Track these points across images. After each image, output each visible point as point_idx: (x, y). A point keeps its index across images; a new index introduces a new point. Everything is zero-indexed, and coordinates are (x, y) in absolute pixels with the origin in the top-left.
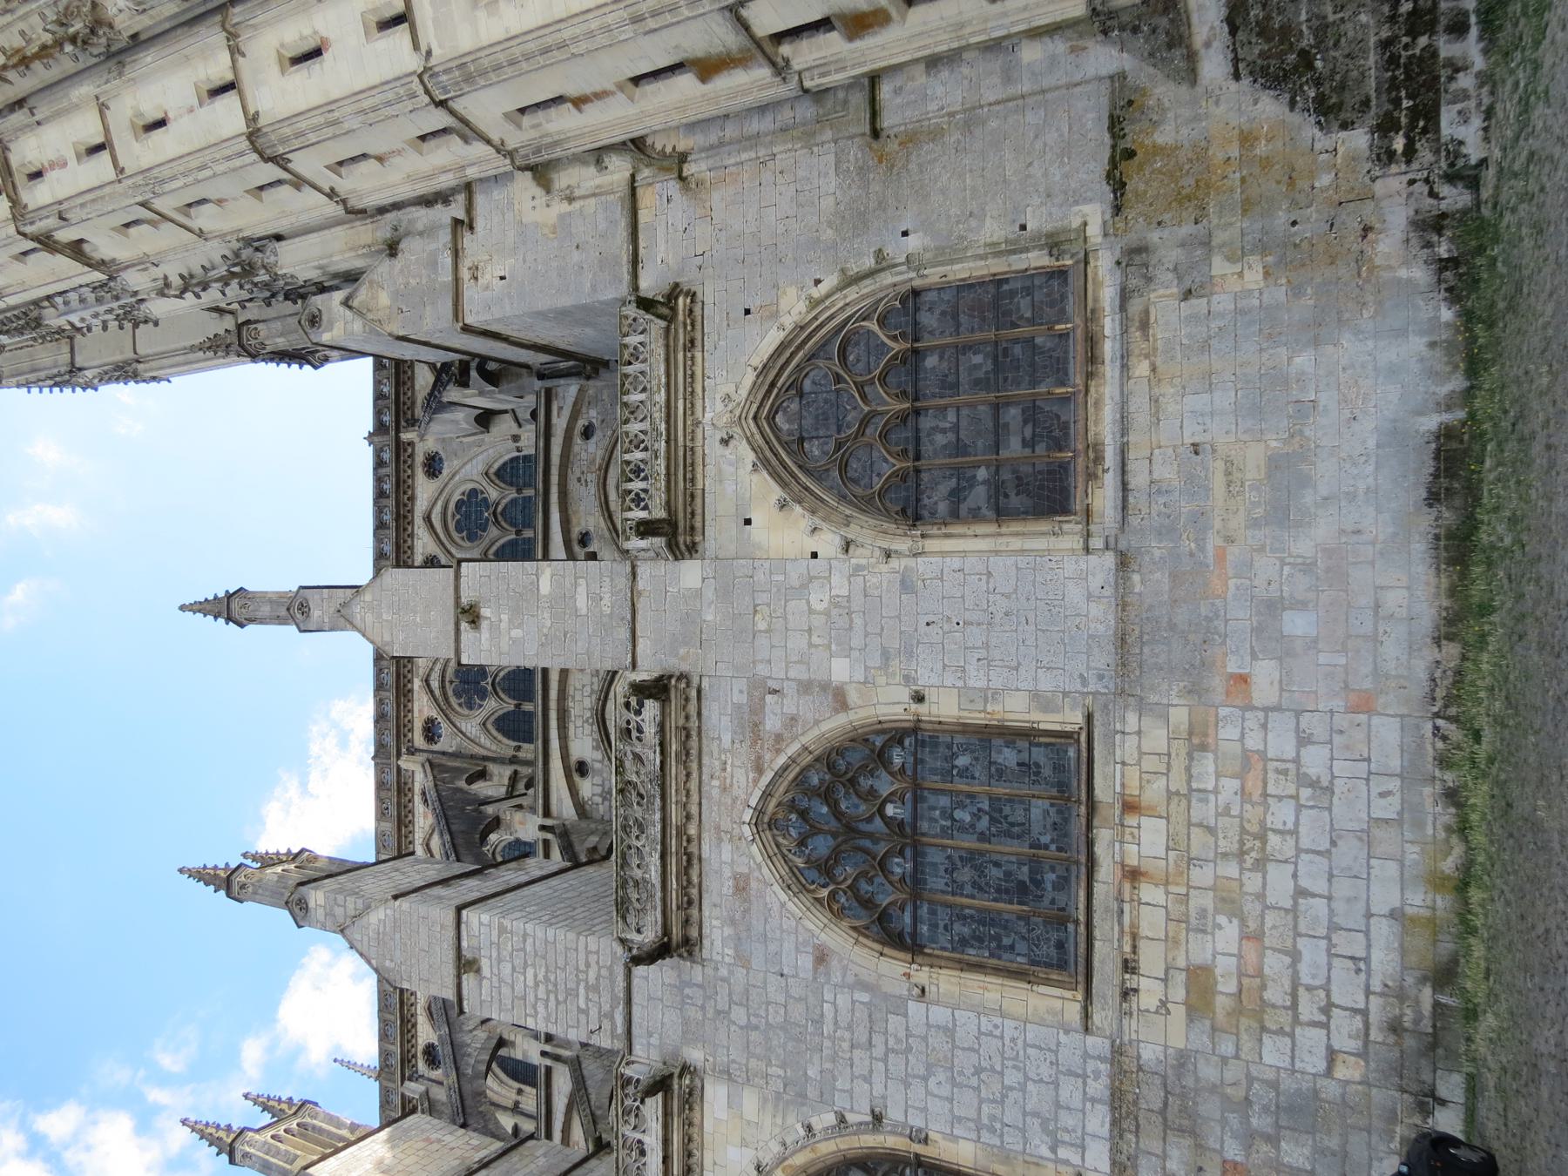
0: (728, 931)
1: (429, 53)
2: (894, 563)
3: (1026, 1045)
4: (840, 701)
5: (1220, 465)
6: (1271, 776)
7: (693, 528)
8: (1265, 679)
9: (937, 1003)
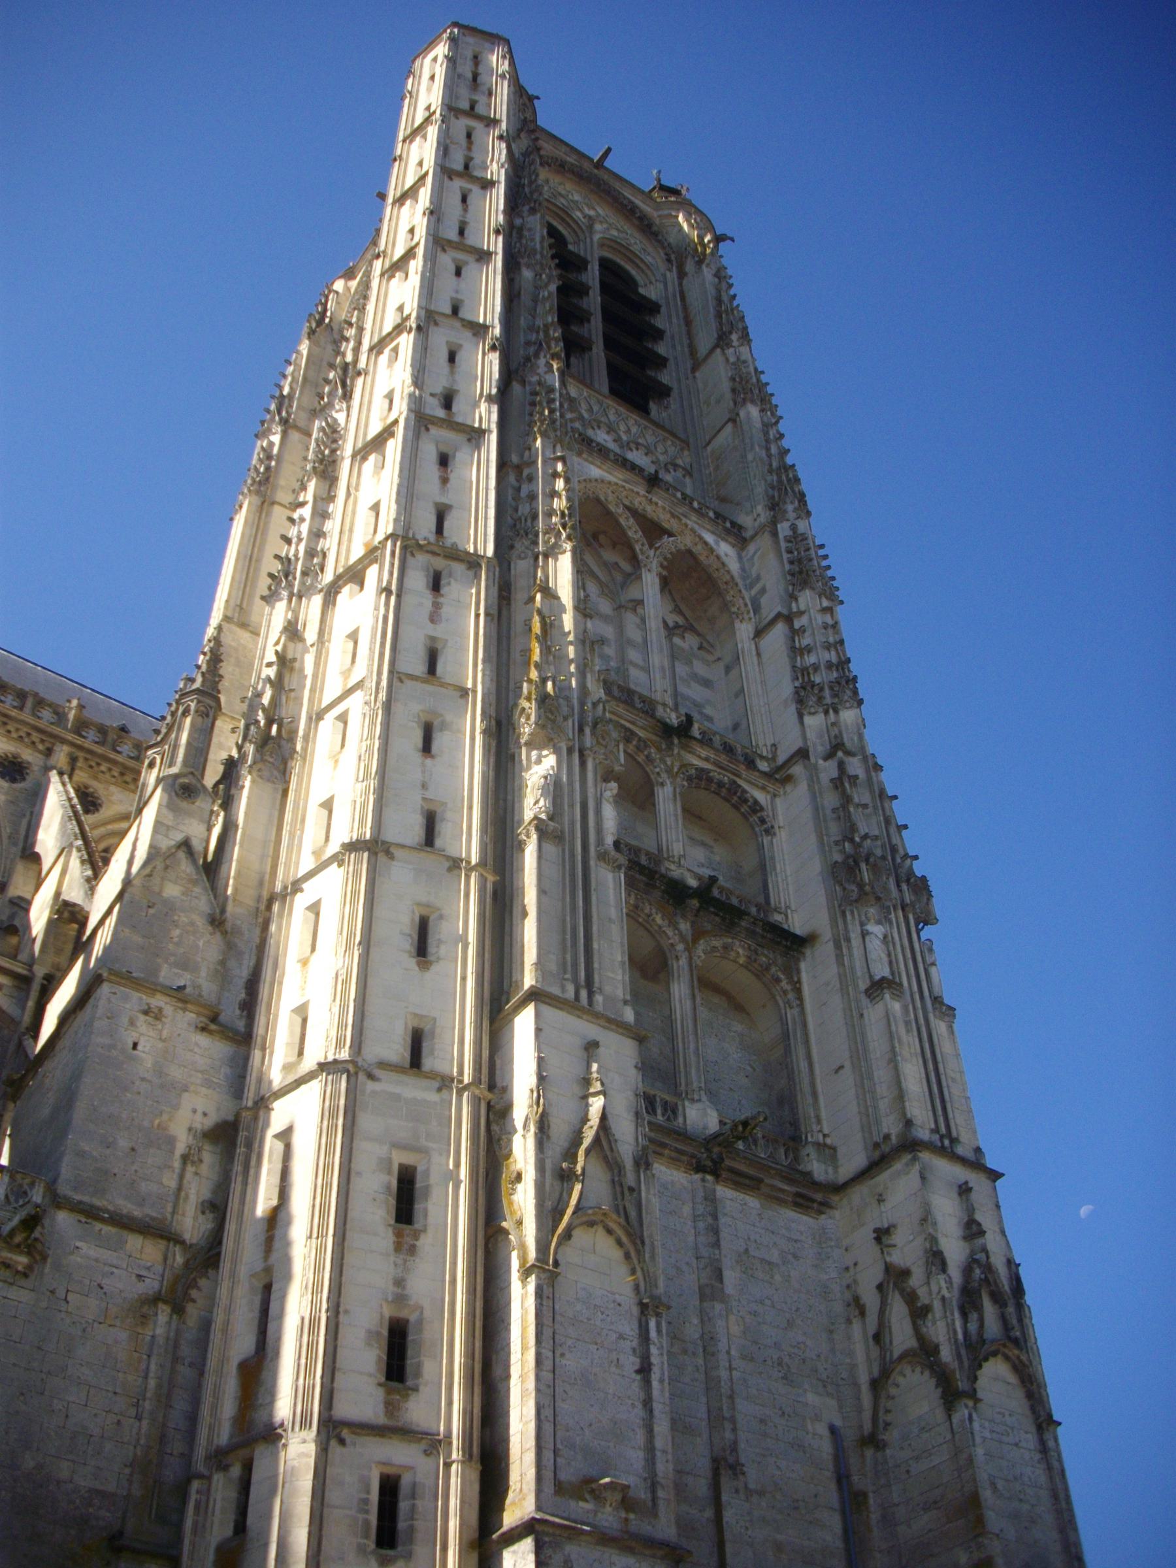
1: (371, 1076)
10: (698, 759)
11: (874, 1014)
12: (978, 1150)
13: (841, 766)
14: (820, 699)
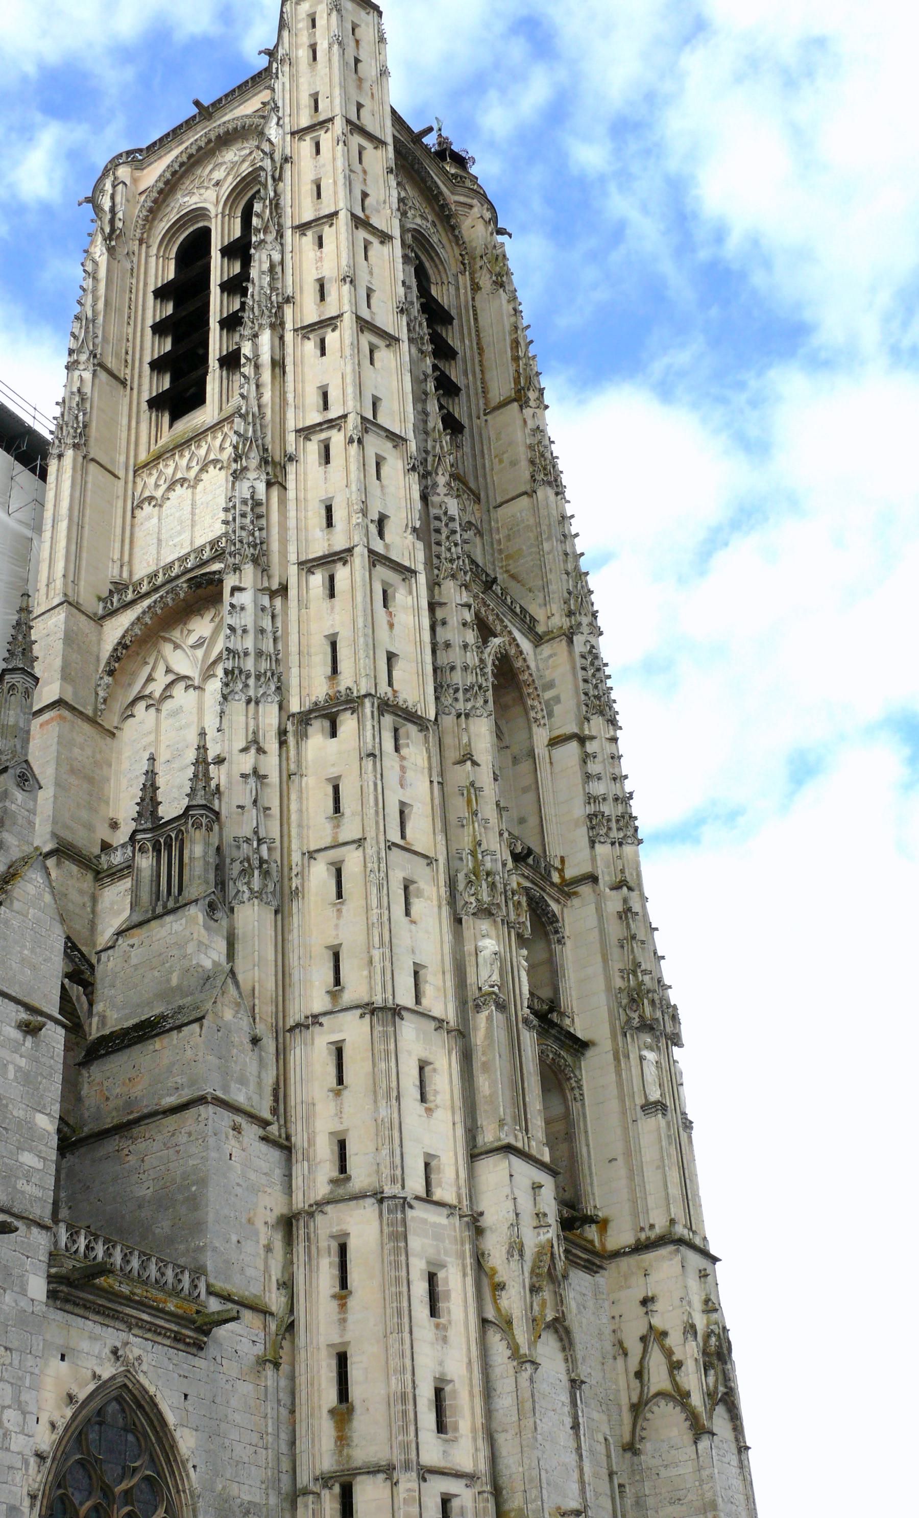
1: (411, 1207)
2: (27, 1502)
7: (67, 1301)
12: (705, 1239)
13: (625, 901)
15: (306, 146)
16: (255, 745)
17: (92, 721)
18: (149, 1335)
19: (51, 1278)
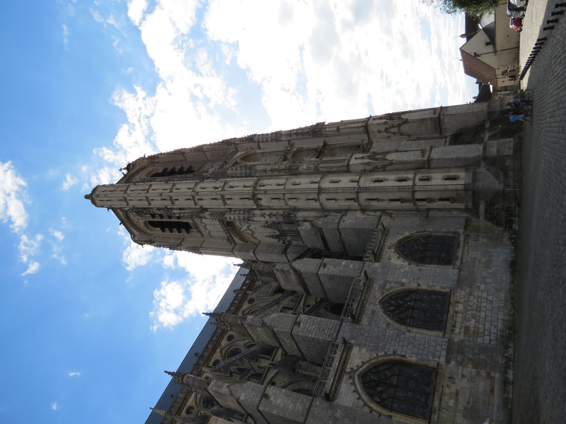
0: (367, 320)
1: (360, 186)
2: (418, 267)
3: (430, 340)
4: (403, 284)
5: (478, 260)
6: (483, 299)
7: (379, 258)
8: (483, 287)
9: (413, 333)
10: (289, 157)
11: (342, 131)
14: (278, 137)
15: (130, 202)
16: (263, 215)
17: (257, 246)
18: (386, 241)
19: (375, 262)
